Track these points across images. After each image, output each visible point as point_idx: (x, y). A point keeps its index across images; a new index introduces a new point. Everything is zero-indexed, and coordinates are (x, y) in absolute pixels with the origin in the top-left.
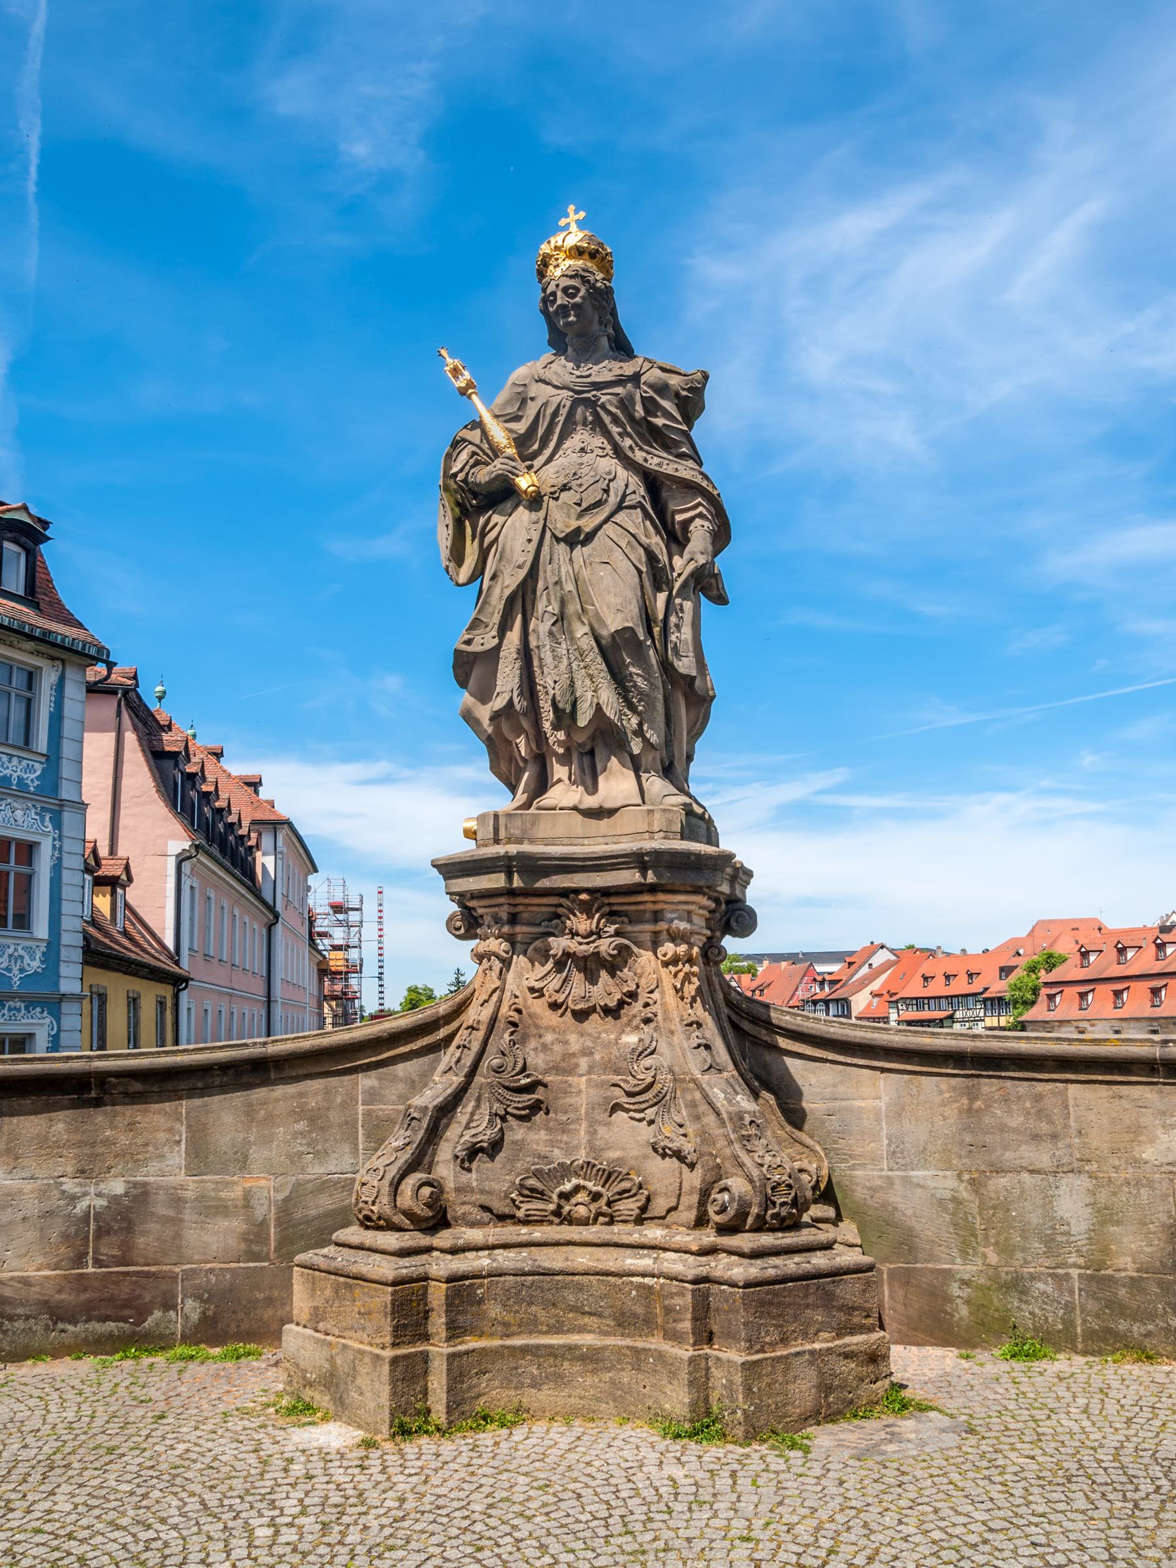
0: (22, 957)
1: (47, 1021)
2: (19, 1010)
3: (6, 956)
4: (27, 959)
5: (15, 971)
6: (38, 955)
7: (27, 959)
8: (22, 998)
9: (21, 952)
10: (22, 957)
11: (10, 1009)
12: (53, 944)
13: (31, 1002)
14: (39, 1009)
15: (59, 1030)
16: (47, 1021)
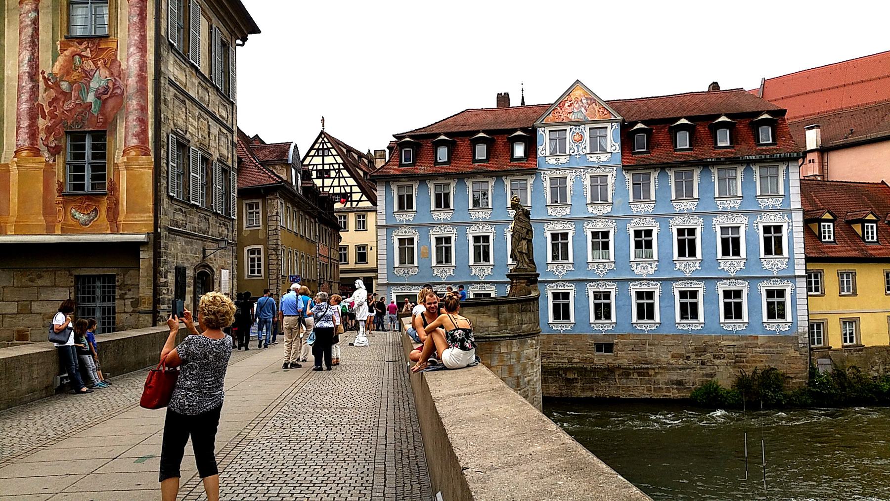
0: (777, 264)
1: (790, 285)
2: (778, 281)
3: (770, 264)
4: (779, 265)
5: (775, 269)
6: (785, 263)
7: (779, 265)
8: (777, 277)
9: (777, 262)
10: (777, 264)
11: (773, 281)
12: (791, 258)
13: (782, 278)
14: (786, 281)
15: (796, 286)
16: (790, 285)
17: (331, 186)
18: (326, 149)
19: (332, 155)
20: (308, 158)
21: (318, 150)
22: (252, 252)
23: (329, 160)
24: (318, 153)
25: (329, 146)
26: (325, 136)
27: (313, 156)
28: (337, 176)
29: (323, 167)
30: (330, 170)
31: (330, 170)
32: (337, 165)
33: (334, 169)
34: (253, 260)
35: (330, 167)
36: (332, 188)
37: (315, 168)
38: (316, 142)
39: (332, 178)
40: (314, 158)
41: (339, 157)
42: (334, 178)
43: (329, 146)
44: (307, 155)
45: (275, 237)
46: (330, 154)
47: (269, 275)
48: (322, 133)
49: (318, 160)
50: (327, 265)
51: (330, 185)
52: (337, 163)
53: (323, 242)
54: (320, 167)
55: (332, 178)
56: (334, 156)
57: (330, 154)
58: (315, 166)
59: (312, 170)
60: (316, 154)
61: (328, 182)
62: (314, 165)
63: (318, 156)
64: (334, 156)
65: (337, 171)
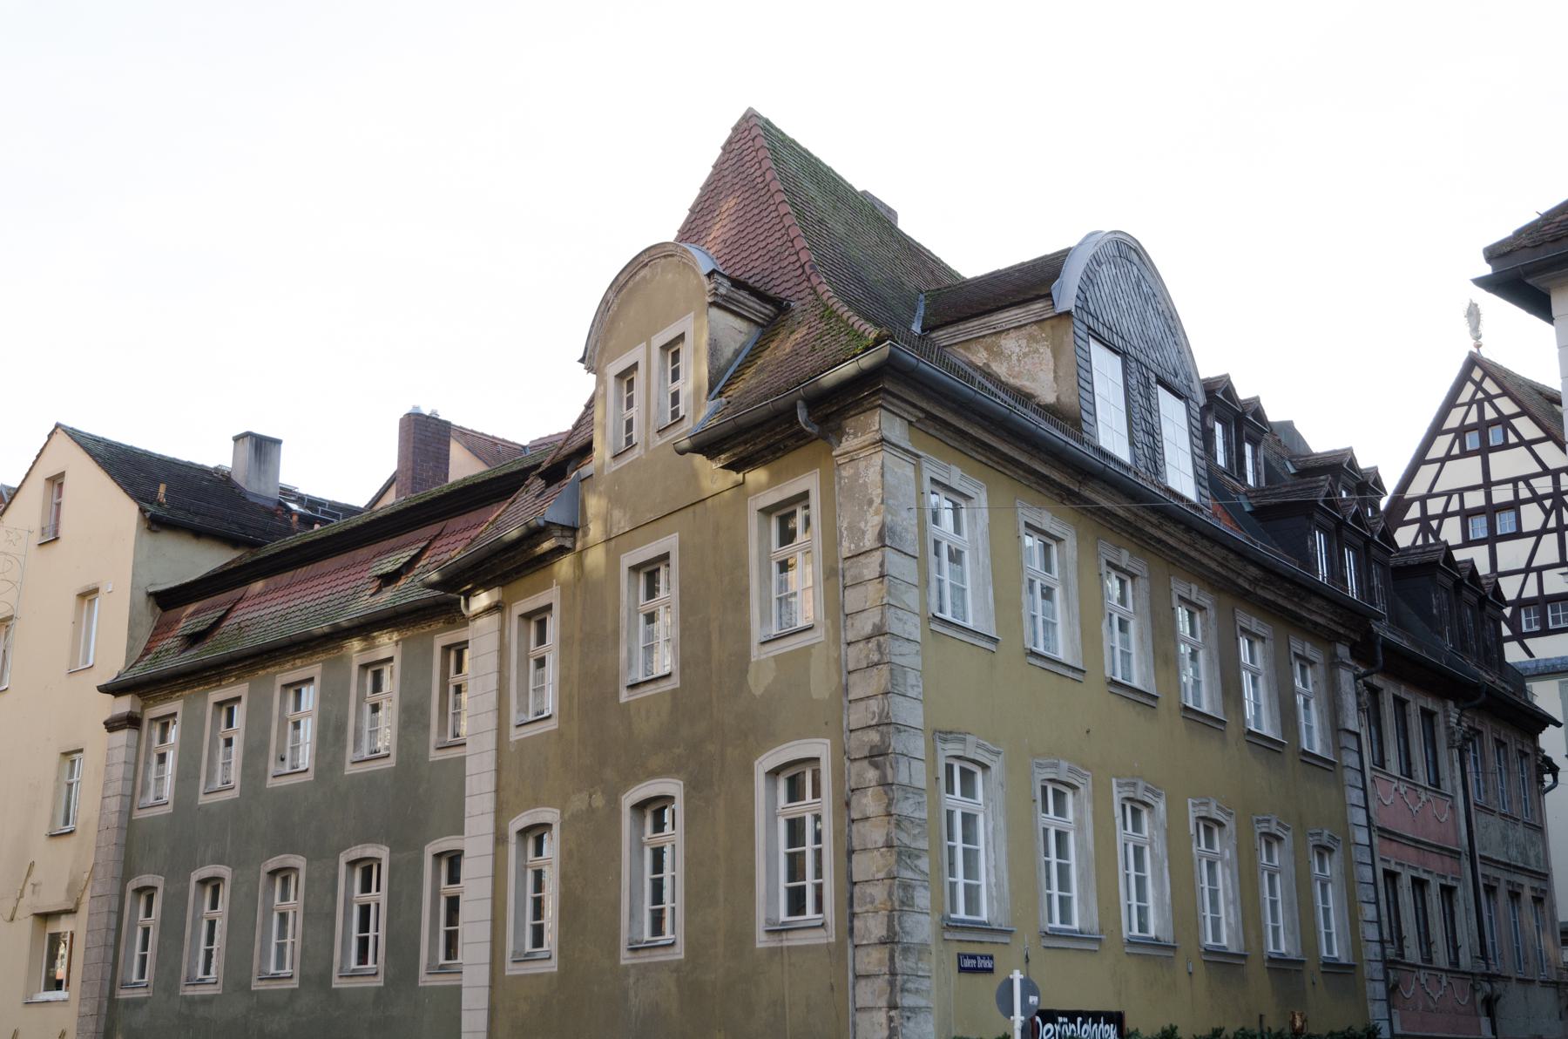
17: (1527, 570)
18: (1493, 423)
19: (1522, 442)
20: (1423, 469)
21: (1461, 432)
22: (794, 778)
23: (1507, 464)
24: (1463, 446)
25: (1507, 406)
26: (1486, 374)
27: (1442, 461)
28: (1552, 523)
29: (1488, 496)
30: (1514, 505)
31: (1514, 505)
32: (1548, 480)
33: (1537, 498)
34: (795, 830)
35: (1516, 493)
36: (1533, 577)
37: (1454, 505)
38: (1450, 403)
39: (1529, 534)
40: (1448, 464)
41: (1550, 445)
42: (1539, 534)
43: (1507, 406)
44: (1420, 460)
45: (876, 681)
46: (1512, 439)
47: (853, 915)
48: (1473, 362)
49: (1466, 472)
50: (1448, 892)
51: (1522, 565)
52: (1546, 471)
53: (1407, 770)
54: (1475, 500)
55: (1529, 534)
56: (1528, 444)
57: (1512, 439)
58: (1456, 498)
59: (1446, 514)
60: (1456, 450)
61: (1512, 554)
62: (1449, 494)
63: (1465, 454)
64: (1528, 444)
65: (1548, 503)
